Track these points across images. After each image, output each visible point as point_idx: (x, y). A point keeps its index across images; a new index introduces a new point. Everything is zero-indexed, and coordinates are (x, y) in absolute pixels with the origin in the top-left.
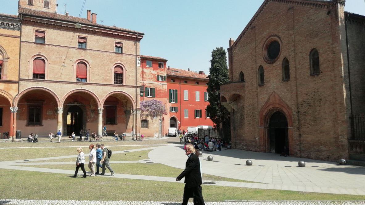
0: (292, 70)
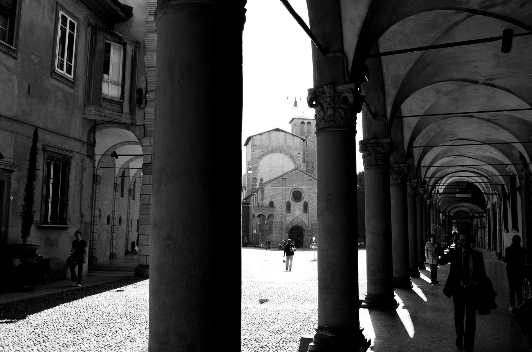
0: (310, 209)
